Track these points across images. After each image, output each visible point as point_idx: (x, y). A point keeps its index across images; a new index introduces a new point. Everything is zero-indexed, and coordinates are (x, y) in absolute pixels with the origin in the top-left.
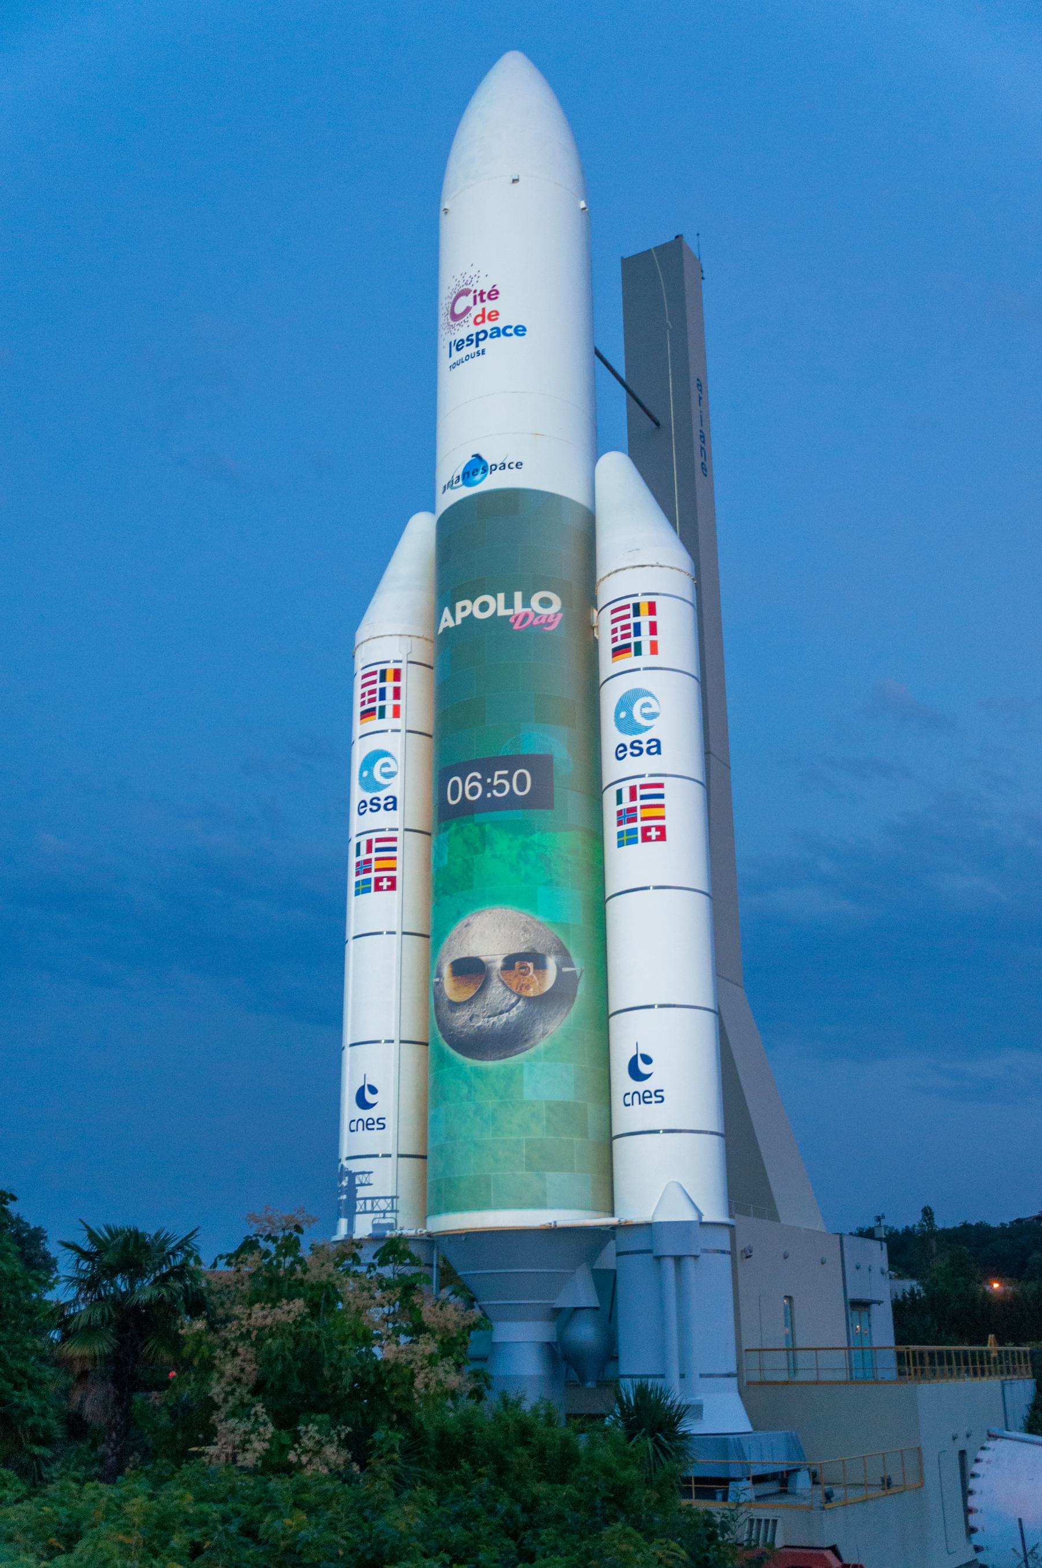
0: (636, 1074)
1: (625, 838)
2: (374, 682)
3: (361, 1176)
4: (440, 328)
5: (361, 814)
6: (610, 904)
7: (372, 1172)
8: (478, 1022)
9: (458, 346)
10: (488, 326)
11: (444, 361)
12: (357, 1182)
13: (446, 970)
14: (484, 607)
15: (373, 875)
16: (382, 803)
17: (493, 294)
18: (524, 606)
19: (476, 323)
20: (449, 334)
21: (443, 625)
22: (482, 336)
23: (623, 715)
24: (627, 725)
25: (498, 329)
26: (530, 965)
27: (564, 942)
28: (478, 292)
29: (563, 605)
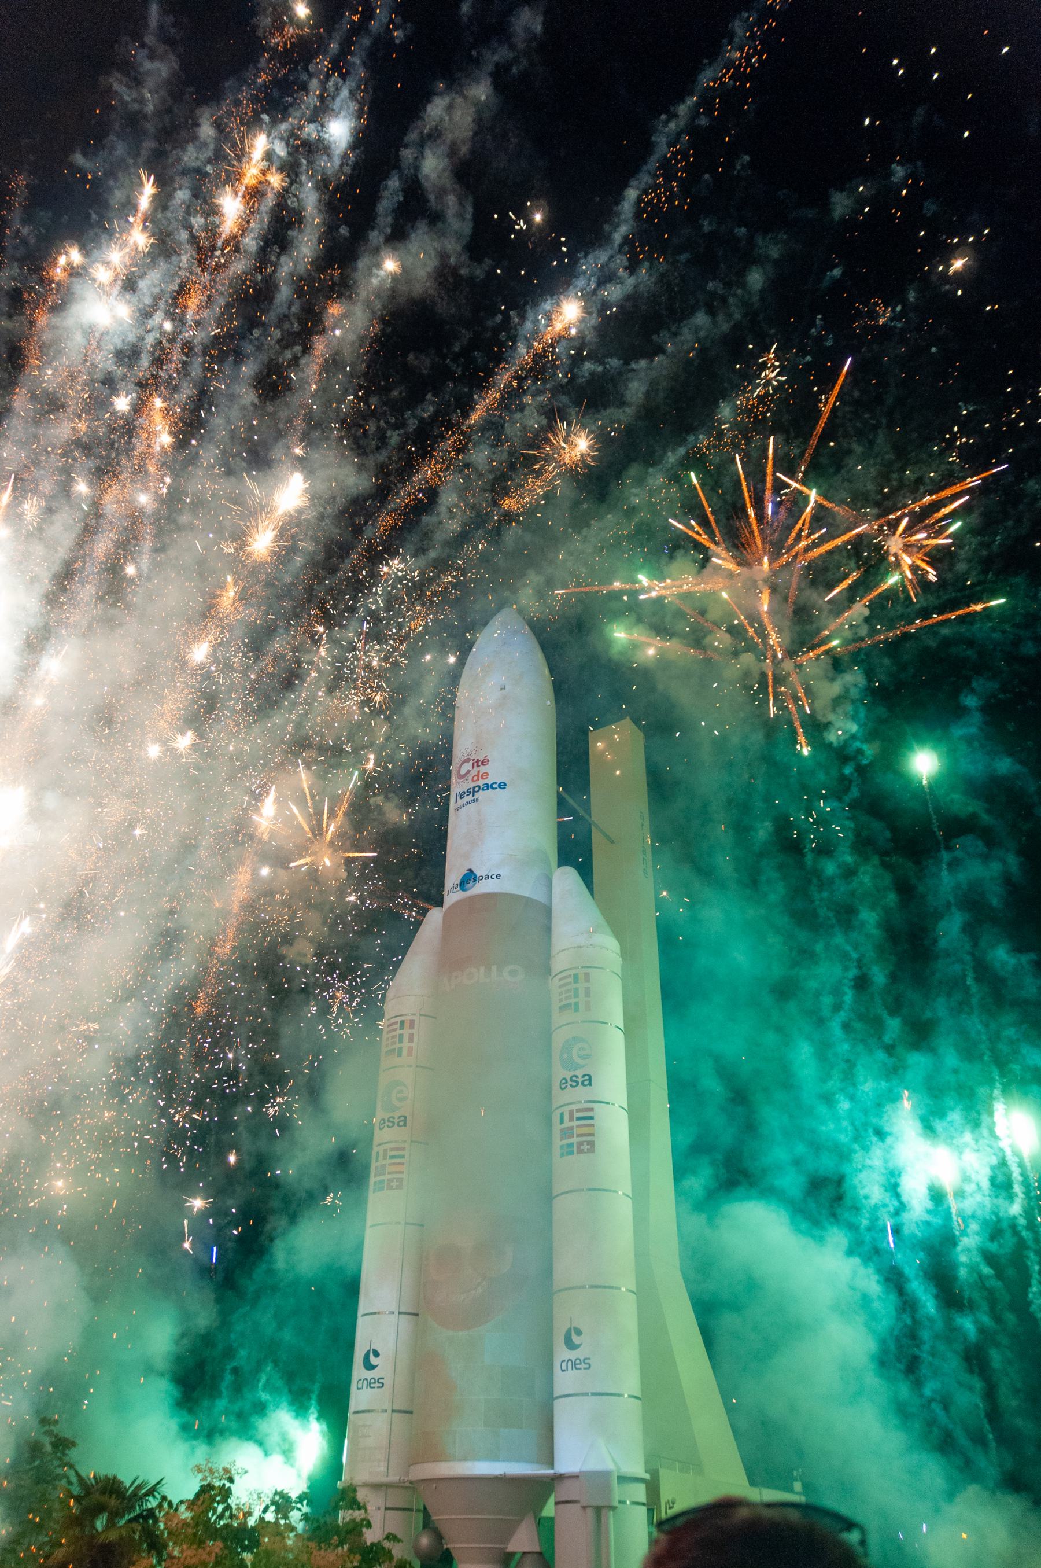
0: (571, 1345)
2: (396, 1030)
5: (381, 1129)
15: (387, 1177)
19: (473, 780)
20: (457, 787)
23: (565, 1056)
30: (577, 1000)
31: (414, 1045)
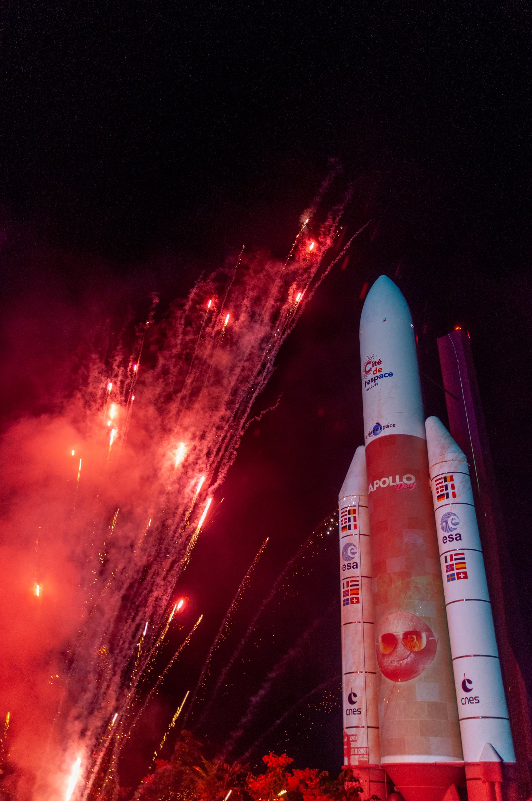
1: (450, 578)
2: (346, 515)
3: (352, 737)
4: (362, 376)
5: (344, 570)
6: (448, 607)
7: (356, 735)
8: (395, 663)
9: (368, 382)
10: (378, 374)
11: (364, 389)
12: (351, 740)
13: (380, 639)
14: (384, 482)
15: (350, 597)
16: (352, 565)
17: (380, 362)
18: (400, 481)
21: (370, 491)
22: (376, 378)
24: (446, 528)
25: (382, 375)
26: (414, 637)
27: (429, 626)
28: (374, 362)
29: (416, 479)
30: (447, 491)
31: (357, 523)
